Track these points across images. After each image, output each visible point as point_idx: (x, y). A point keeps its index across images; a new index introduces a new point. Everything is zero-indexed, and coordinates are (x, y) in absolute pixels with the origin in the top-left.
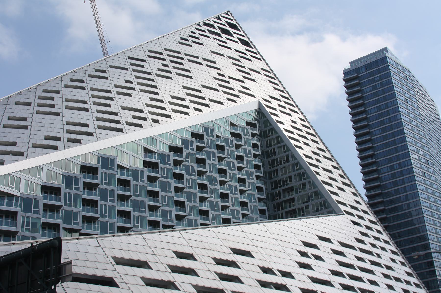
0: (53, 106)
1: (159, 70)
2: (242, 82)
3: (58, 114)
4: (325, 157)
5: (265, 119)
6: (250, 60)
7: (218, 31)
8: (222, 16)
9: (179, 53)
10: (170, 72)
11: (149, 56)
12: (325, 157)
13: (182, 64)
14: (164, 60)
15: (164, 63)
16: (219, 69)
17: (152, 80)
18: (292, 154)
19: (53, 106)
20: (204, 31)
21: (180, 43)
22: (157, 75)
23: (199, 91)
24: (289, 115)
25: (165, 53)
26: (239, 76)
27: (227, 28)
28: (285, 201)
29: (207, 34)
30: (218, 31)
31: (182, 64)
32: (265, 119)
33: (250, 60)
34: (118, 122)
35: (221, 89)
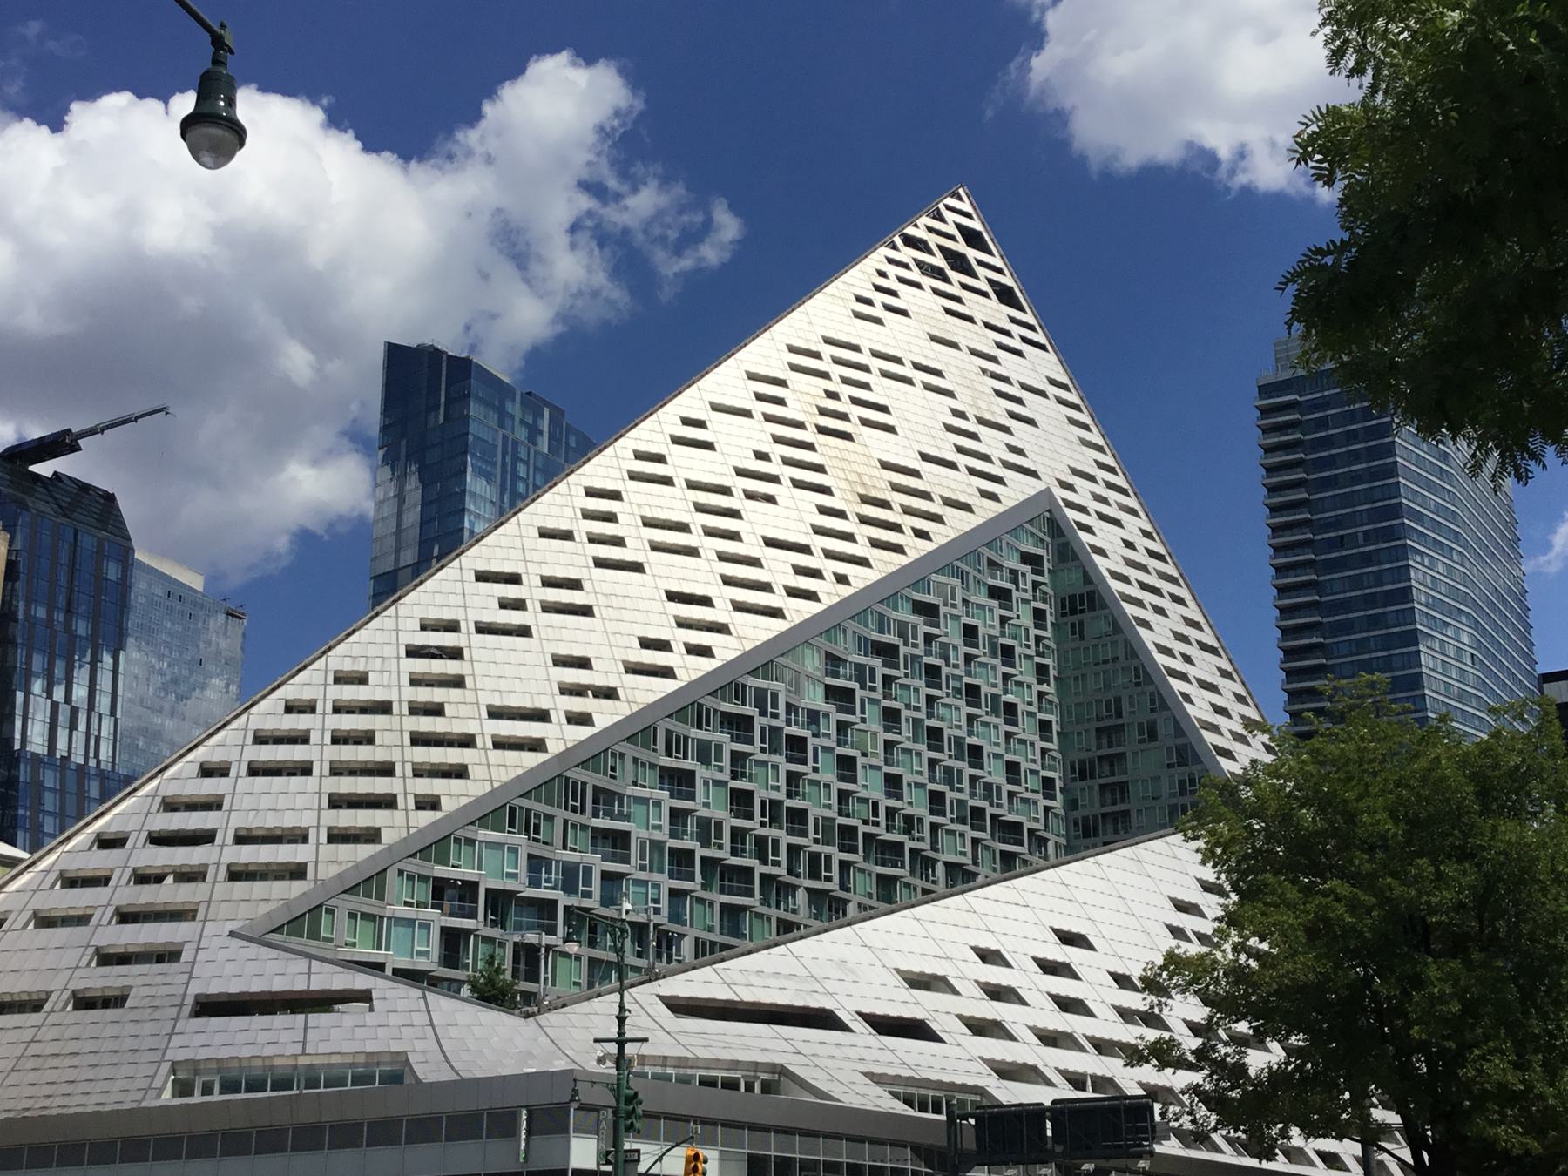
0: (618, 542)
1: (823, 412)
2: (1006, 430)
3: (637, 567)
4: (1204, 647)
5: (1062, 540)
6: (1019, 353)
7: (938, 261)
8: (948, 208)
9: (856, 348)
10: (844, 417)
11: (795, 368)
12: (1204, 647)
13: (866, 386)
14: (825, 375)
15: (831, 387)
16: (949, 394)
17: (809, 447)
18: (1126, 642)
19: (618, 542)
20: (906, 266)
21: (857, 315)
22: (822, 430)
23: (915, 473)
24: (1117, 523)
25: (828, 351)
26: (999, 410)
27: (960, 246)
28: (1100, 758)
29: (915, 275)
30: (938, 261)
31: (866, 386)
32: (1062, 540)
33: (1019, 353)
34: (765, 587)
35: (963, 461)
